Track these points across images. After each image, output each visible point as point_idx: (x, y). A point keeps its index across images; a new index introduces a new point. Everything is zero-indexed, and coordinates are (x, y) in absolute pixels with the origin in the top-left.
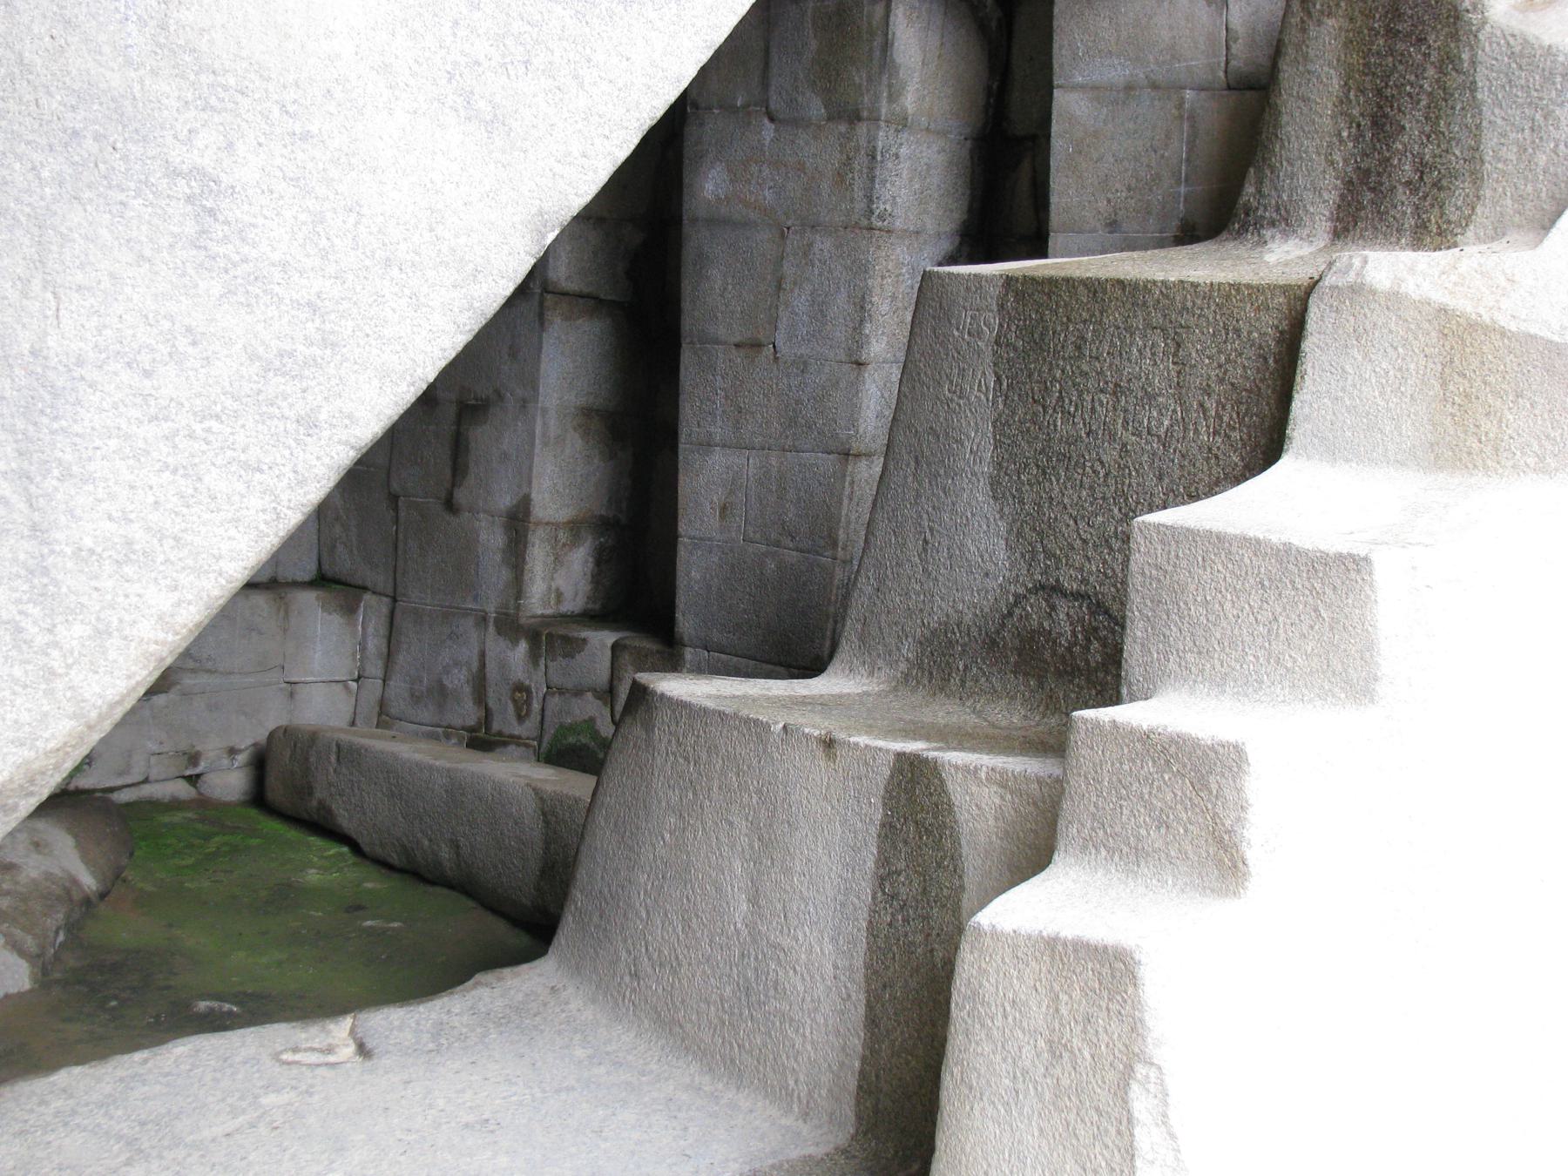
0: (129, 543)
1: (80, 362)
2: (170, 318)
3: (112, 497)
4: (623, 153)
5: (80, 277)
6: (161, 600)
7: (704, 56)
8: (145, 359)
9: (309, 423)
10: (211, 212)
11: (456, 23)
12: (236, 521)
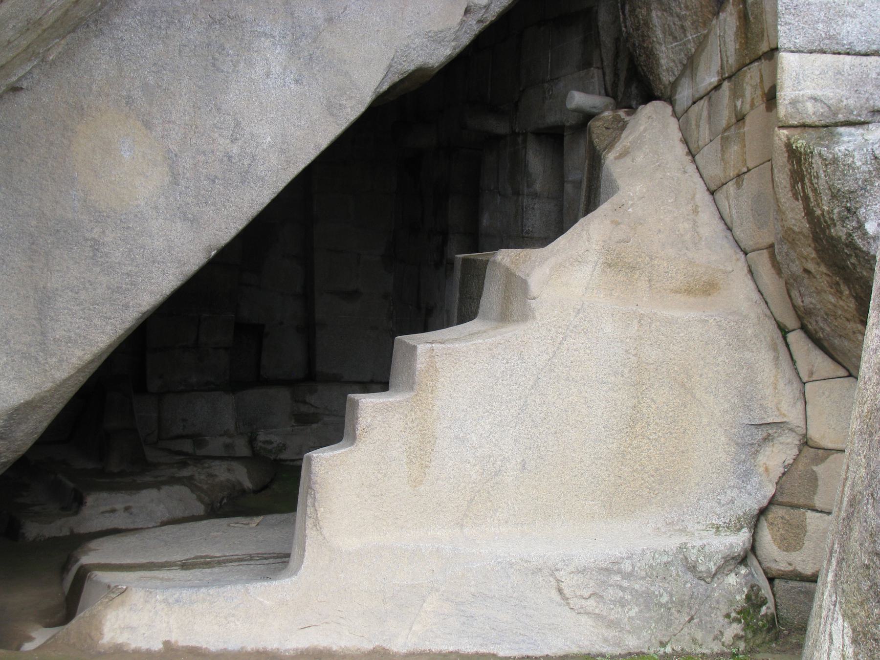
0: (70, 337)
1: (57, 290)
2: (84, 278)
3: (65, 325)
4: (241, 228)
5: (58, 268)
6: (79, 353)
7: (273, 196)
8: (76, 289)
9: (126, 306)
10: (97, 250)
11: (181, 193)
12: (103, 333)
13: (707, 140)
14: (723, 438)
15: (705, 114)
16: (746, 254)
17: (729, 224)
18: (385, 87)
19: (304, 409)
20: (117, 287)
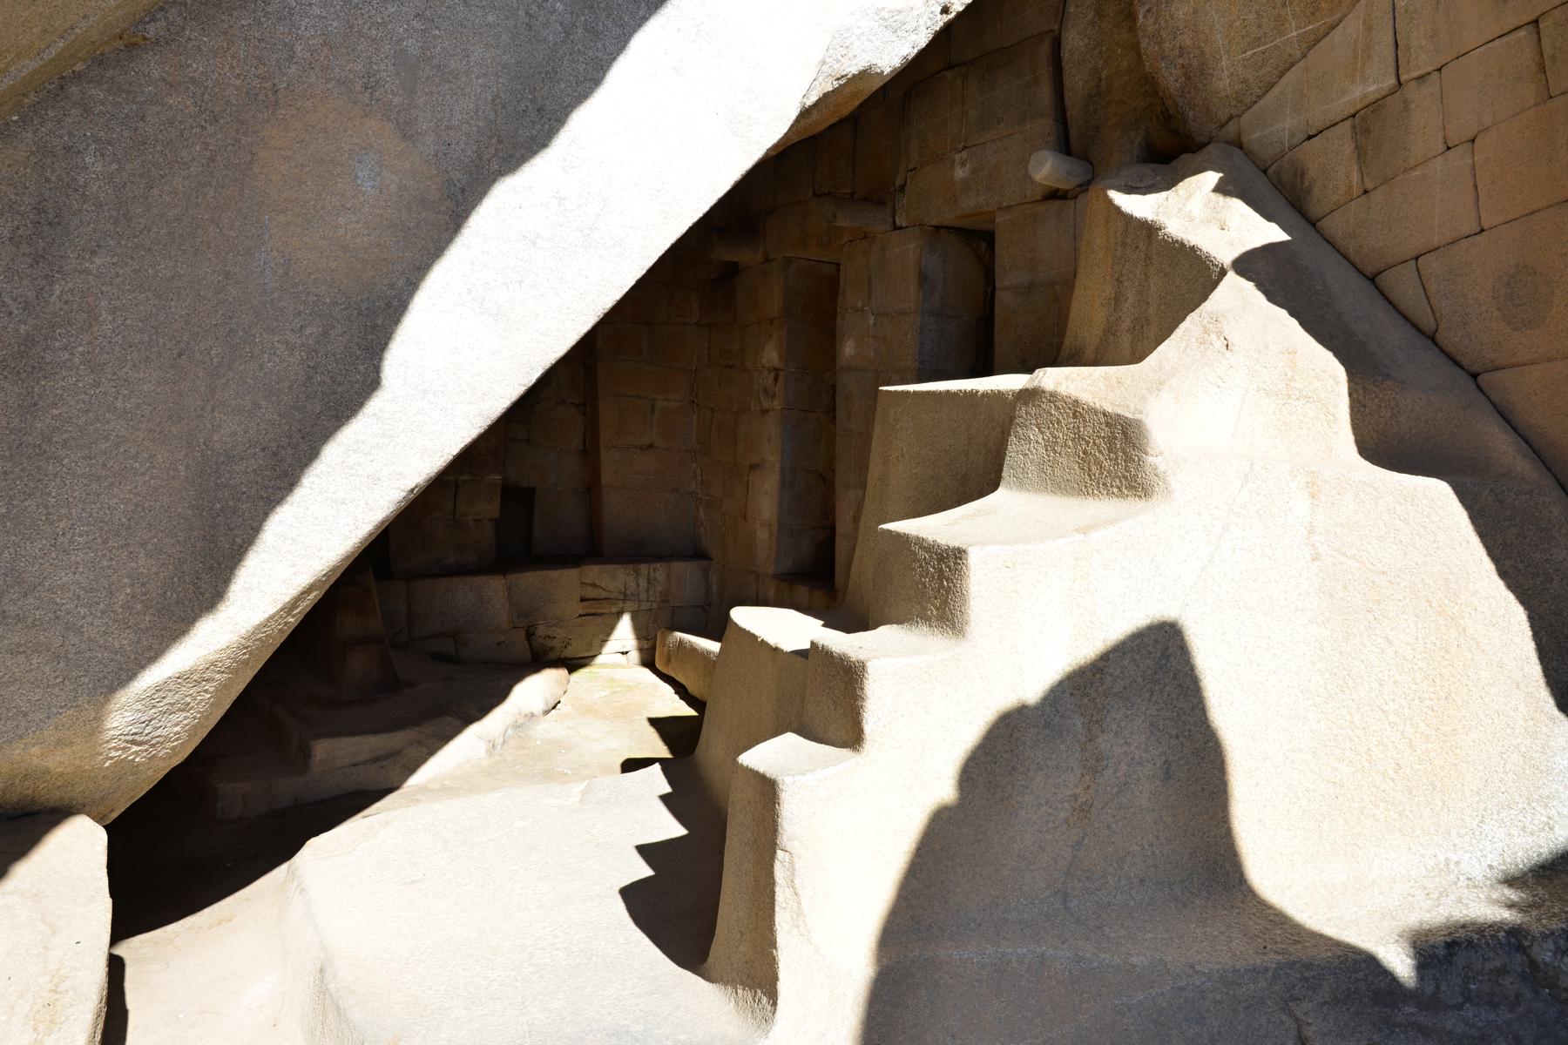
13: (1356, 191)
14: (1522, 708)
15: (1348, 148)
16: (1475, 376)
17: (1428, 323)
18: (813, 99)
19: (590, 593)
20: (357, 442)
